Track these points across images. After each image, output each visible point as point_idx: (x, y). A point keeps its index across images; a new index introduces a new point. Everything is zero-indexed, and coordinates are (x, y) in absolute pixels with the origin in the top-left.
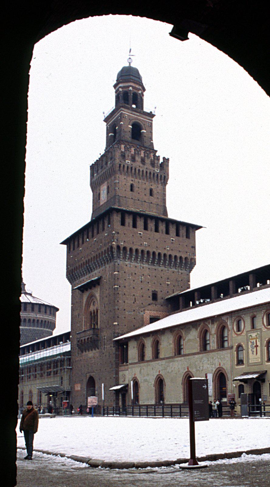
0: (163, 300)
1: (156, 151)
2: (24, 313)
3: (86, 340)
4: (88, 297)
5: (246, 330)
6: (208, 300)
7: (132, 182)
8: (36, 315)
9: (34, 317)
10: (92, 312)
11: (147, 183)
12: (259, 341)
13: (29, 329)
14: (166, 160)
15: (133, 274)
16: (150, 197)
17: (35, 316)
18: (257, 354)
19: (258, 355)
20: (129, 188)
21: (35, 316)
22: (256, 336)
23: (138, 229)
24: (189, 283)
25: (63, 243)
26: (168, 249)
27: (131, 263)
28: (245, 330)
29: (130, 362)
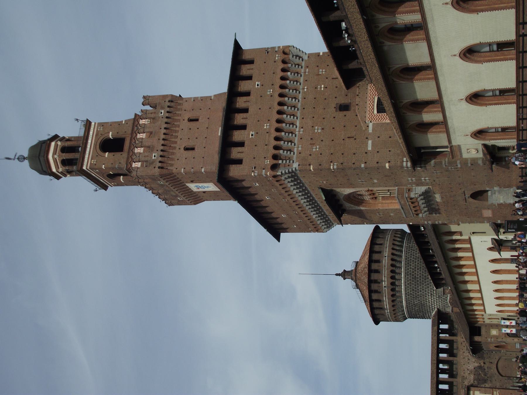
1: (136, 115)
2: (384, 273)
4: (352, 203)
6: (344, 25)
8: (385, 257)
11: (181, 127)
14: (147, 100)
16: (200, 121)
17: (386, 258)
20: (190, 152)
21: (386, 258)
23: (245, 139)
24: (321, 54)
25: (278, 238)
26: (271, 90)
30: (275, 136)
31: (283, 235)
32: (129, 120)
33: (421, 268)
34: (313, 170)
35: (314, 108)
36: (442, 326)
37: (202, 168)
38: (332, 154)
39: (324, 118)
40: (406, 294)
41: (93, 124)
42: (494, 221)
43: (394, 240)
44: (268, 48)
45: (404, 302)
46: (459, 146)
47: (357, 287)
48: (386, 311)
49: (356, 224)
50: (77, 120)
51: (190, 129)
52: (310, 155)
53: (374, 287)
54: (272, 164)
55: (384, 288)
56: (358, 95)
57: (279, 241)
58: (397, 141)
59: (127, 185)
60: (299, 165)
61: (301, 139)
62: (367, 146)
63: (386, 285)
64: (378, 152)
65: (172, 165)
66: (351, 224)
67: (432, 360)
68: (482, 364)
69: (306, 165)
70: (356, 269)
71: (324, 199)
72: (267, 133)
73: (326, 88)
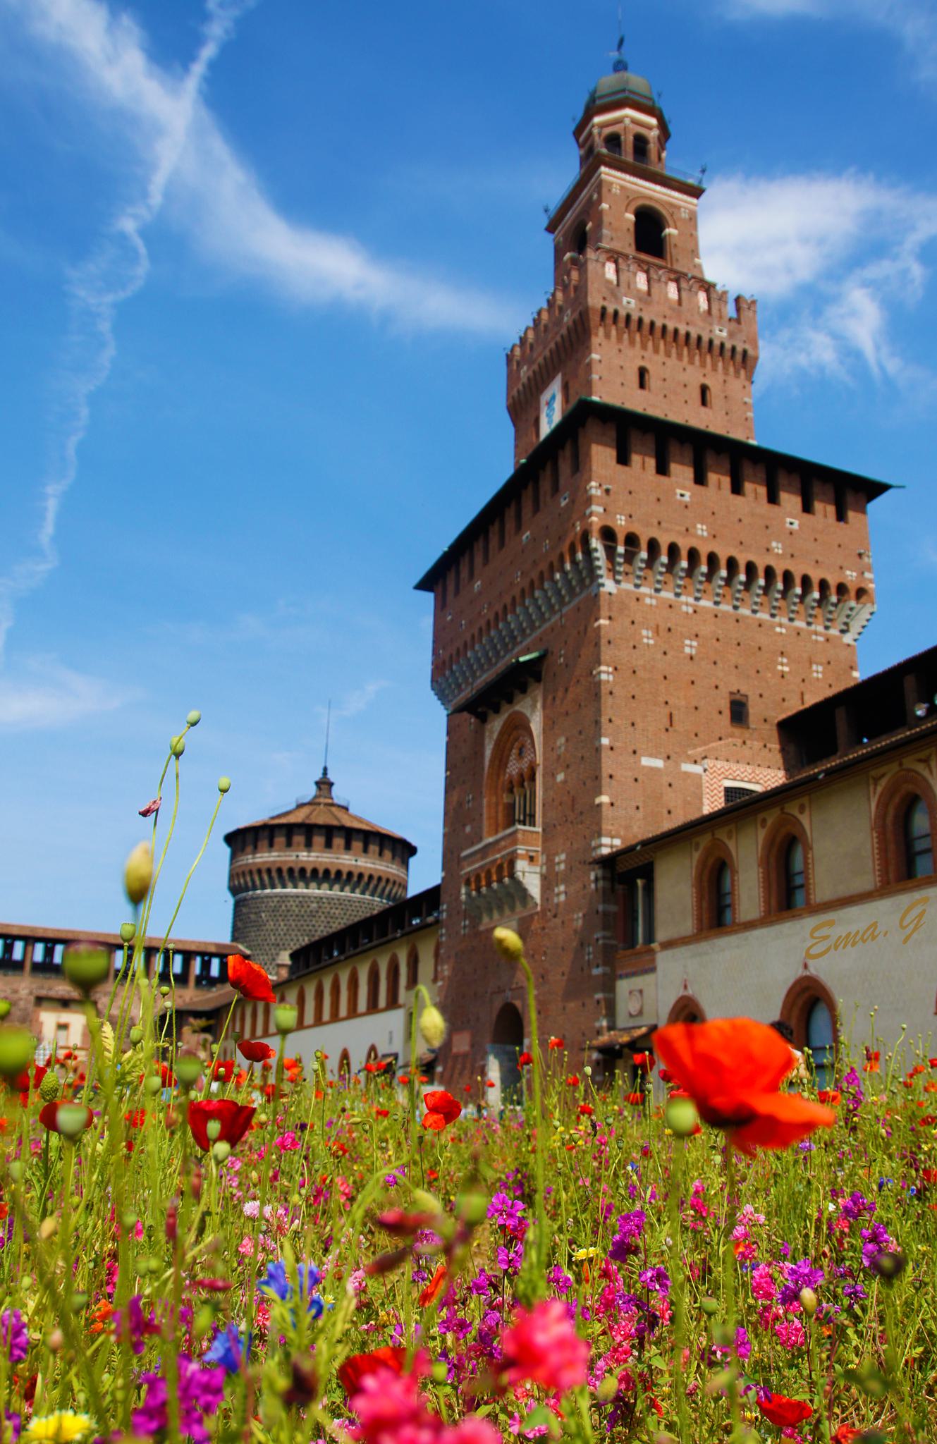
7: (642, 363)
11: (690, 368)
15: (663, 627)
16: (703, 409)
21: (354, 862)
23: (673, 479)
29: (662, 935)
32: (701, 272)
35: (739, 644)
38: (634, 672)
39: (715, 663)
41: (694, 201)
43: (388, 881)
46: (653, 970)
47: (300, 806)
48: (250, 856)
49: (447, 753)
52: (633, 623)
54: (617, 530)
55: (294, 854)
56: (765, 746)
60: (610, 594)
61: (671, 606)
62: (651, 755)
63: (301, 858)
64: (636, 780)
65: (607, 336)
66: (448, 744)
69: (610, 609)
71: (522, 659)
72: (687, 530)
73: (783, 677)
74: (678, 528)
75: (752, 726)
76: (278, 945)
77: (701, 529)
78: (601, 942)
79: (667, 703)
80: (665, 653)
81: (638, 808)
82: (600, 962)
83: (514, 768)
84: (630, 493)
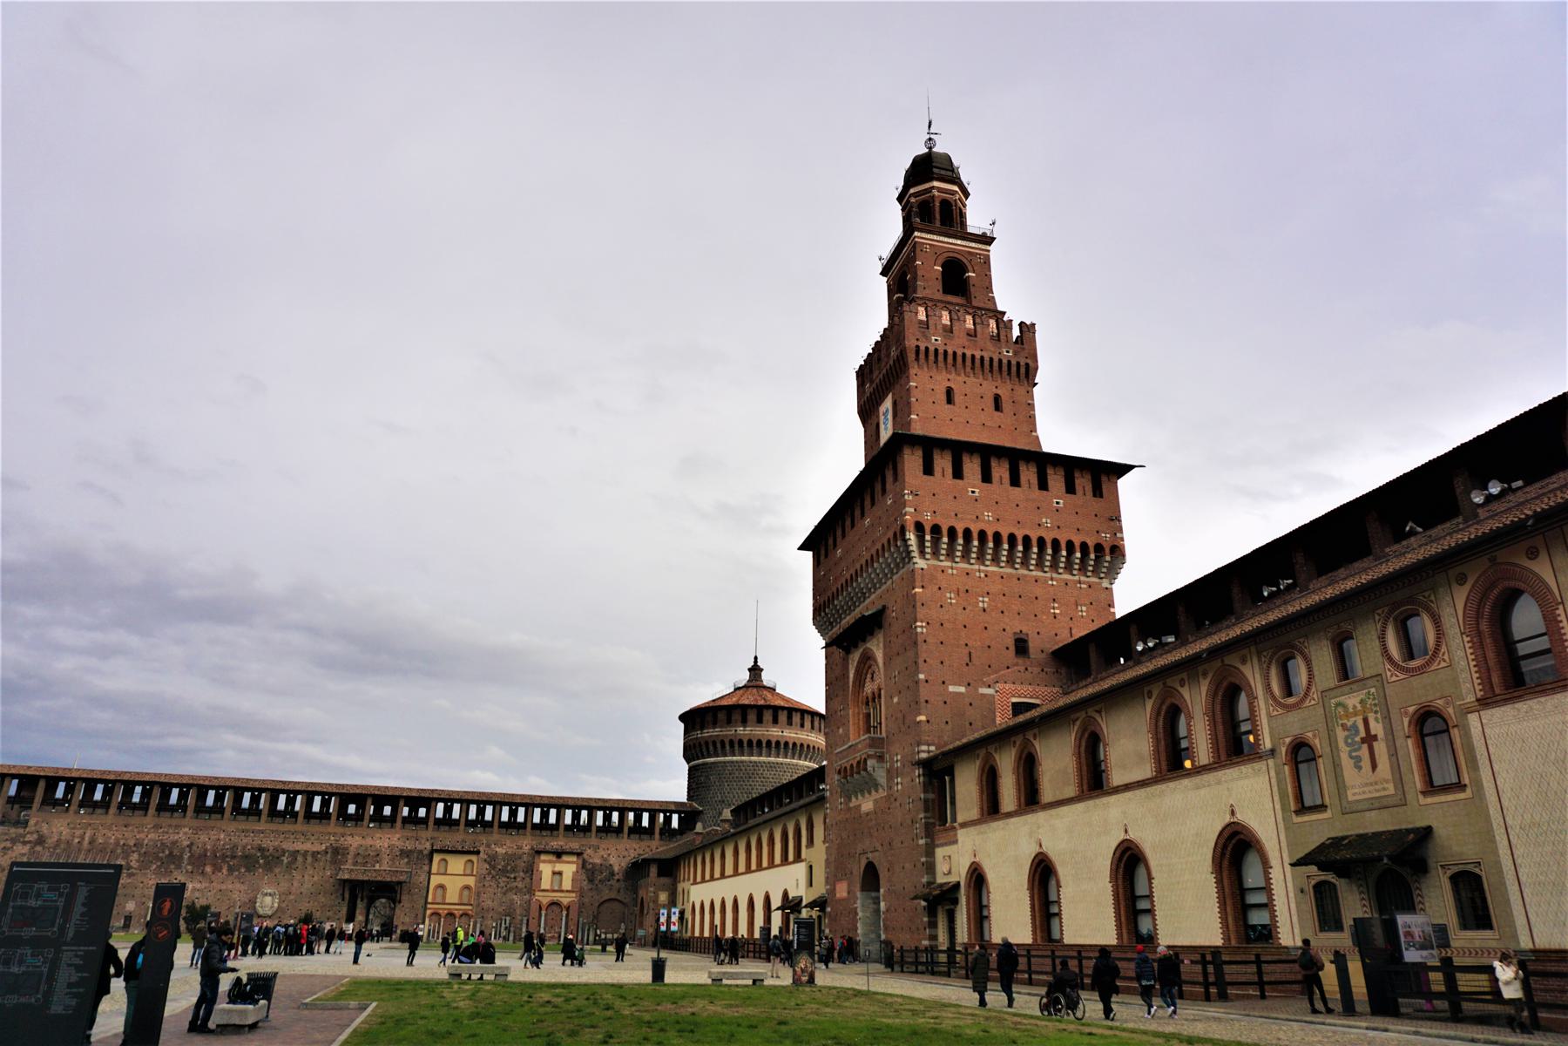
0: (1044, 655)
1: (1004, 313)
3: (855, 765)
5: (1320, 689)
6: (1171, 639)
7: (949, 384)
9: (777, 736)
10: (870, 696)
11: (985, 383)
12: (1376, 719)
13: (769, 763)
14: (1028, 329)
15: (962, 589)
17: (781, 733)
18: (1374, 766)
19: (1378, 769)
20: (944, 397)
21: (781, 733)
22: (1362, 702)
23: (965, 480)
24: (1112, 610)
25: (802, 548)
26: (1049, 525)
27: (954, 565)
28: (1313, 689)
29: (960, 818)
30: (972, 529)
31: (809, 554)
32: (995, 304)
33: (764, 786)
34: (913, 592)
36: (675, 817)
37: (917, 415)
38: (942, 624)
39: (1002, 612)
40: (724, 762)
41: (988, 248)
42: (828, 900)
44: (1120, 521)
45: (712, 760)
46: (956, 842)
47: (737, 689)
49: (826, 672)
50: (994, 223)
51: (982, 397)
52: (940, 588)
53: (737, 716)
54: (924, 524)
55: (734, 729)
56: (1043, 670)
57: (799, 549)
58: (963, 736)
59: (889, 305)
60: (922, 569)
61: (968, 574)
62: (955, 684)
63: (738, 732)
64: (945, 703)
66: (826, 665)
67: (624, 800)
68: (617, 877)
69: (922, 581)
70: (765, 687)
72: (977, 517)
73: (1055, 617)
74: (969, 517)
75: (1032, 656)
76: (723, 801)
77: (988, 516)
78: (923, 821)
79: (967, 645)
80: (964, 609)
81: (947, 723)
82: (923, 835)
83: (869, 688)
84: (934, 495)
